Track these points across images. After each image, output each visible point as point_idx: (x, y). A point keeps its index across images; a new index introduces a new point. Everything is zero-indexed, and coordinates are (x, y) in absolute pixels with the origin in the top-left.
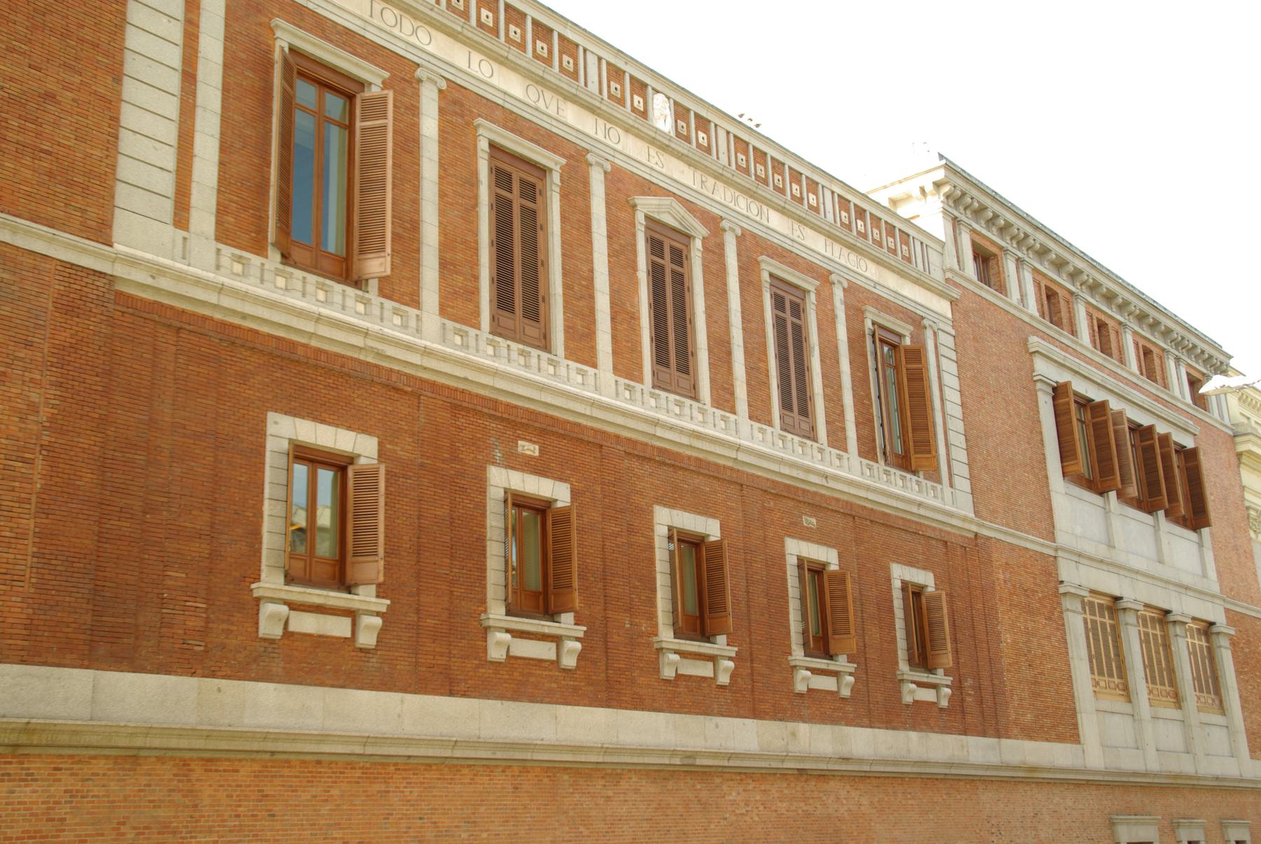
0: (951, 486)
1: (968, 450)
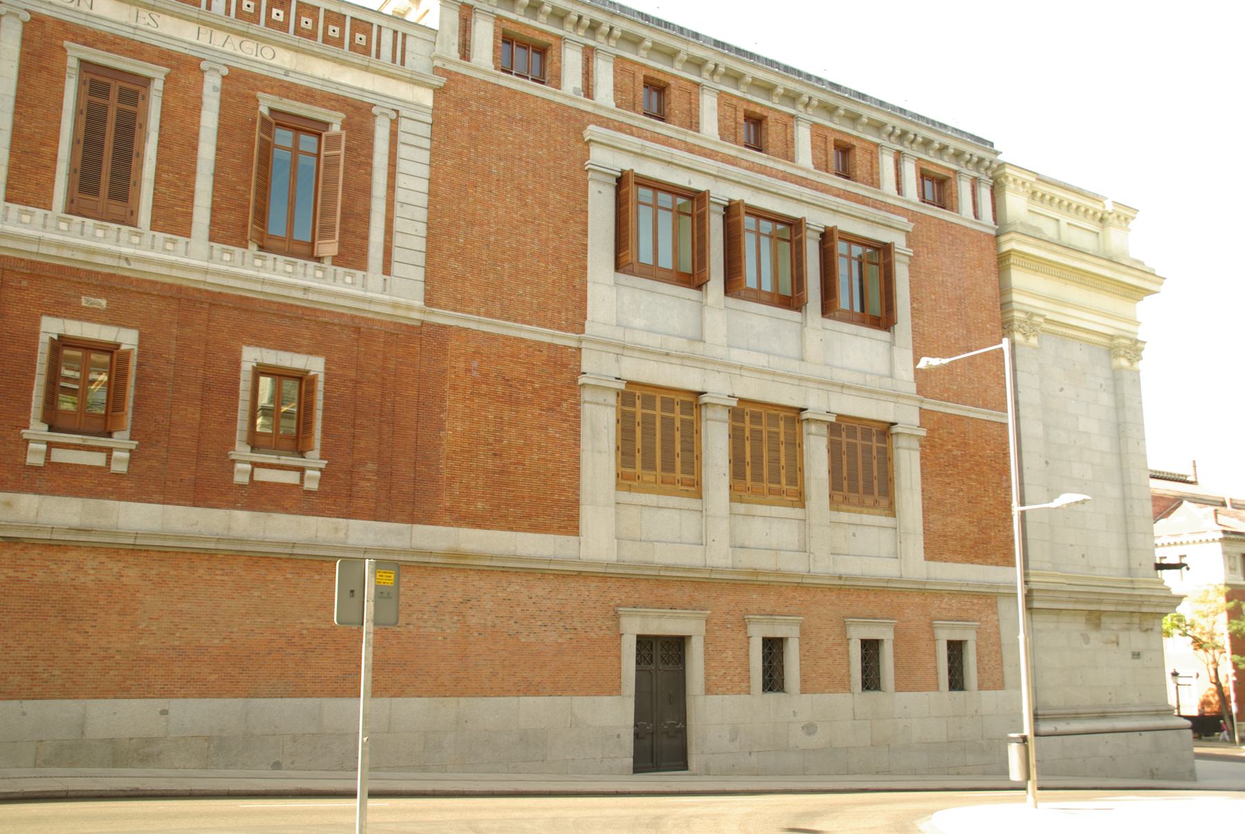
0: (387, 270)
1: (431, 238)
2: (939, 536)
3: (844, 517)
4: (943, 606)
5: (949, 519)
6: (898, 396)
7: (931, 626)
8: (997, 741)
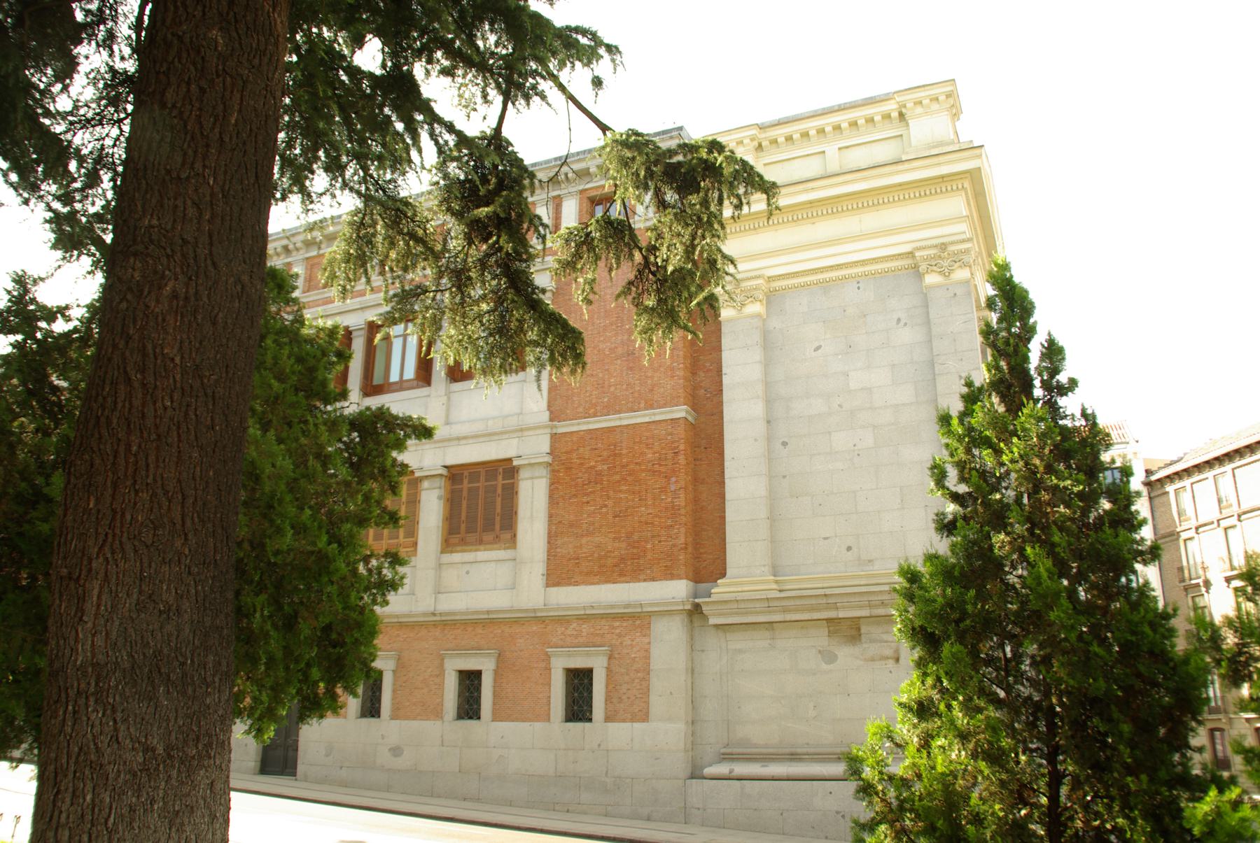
2: (570, 559)
3: (457, 557)
4: (569, 632)
5: (584, 540)
6: (522, 430)
7: (548, 657)
8: (628, 781)
